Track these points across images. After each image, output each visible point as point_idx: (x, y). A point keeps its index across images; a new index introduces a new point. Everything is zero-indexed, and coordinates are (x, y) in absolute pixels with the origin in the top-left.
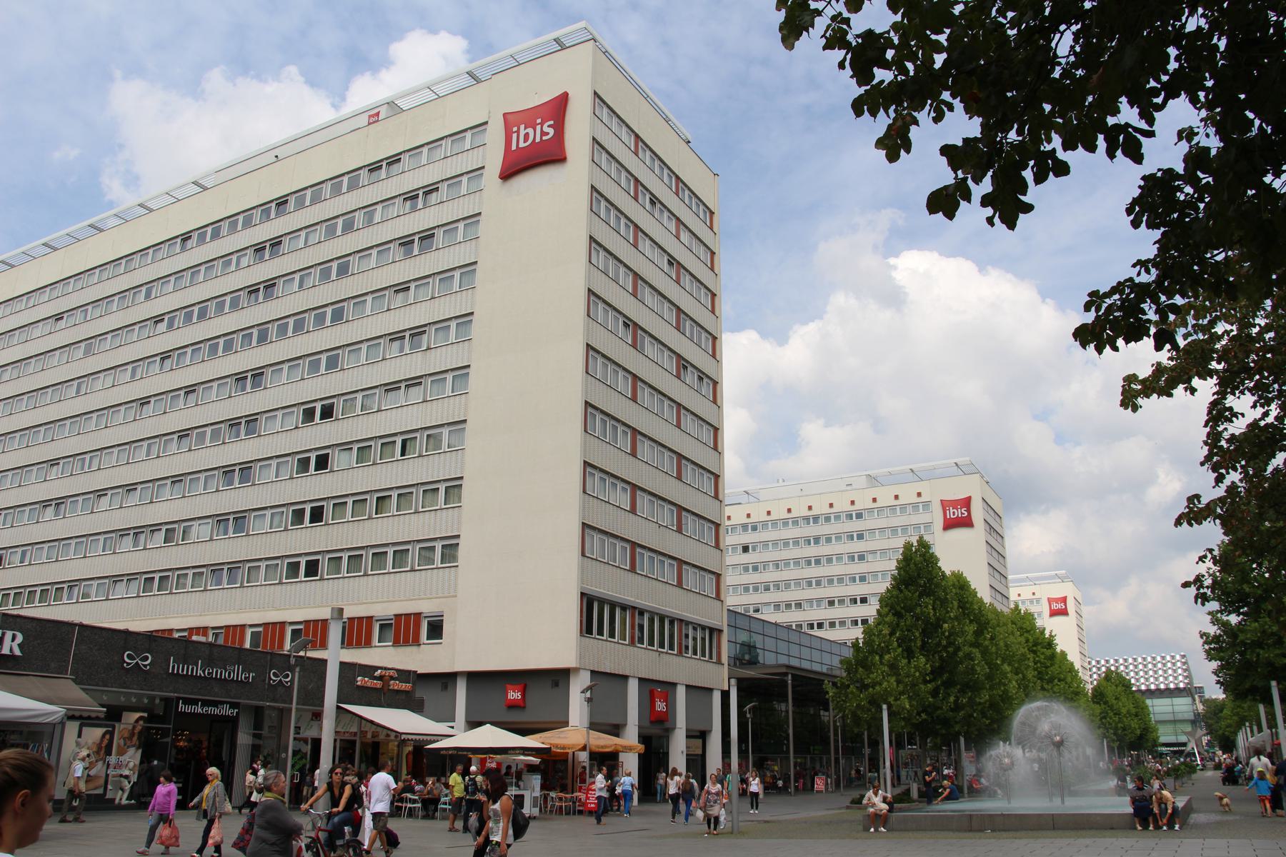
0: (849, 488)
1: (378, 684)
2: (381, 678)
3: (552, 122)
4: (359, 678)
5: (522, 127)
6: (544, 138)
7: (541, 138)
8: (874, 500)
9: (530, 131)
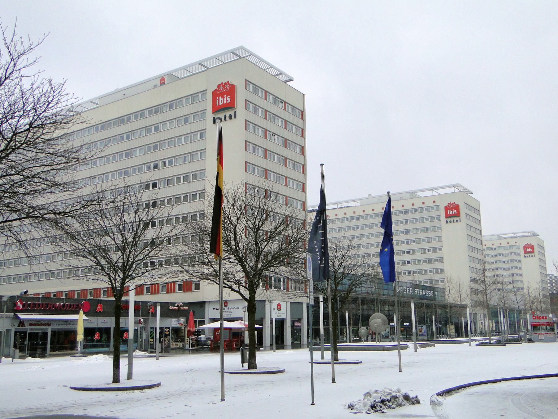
0: (401, 199)
1: (177, 308)
2: (178, 306)
3: (229, 97)
4: (170, 307)
5: (220, 97)
6: (227, 102)
7: (226, 102)
8: (413, 205)
9: (222, 99)
